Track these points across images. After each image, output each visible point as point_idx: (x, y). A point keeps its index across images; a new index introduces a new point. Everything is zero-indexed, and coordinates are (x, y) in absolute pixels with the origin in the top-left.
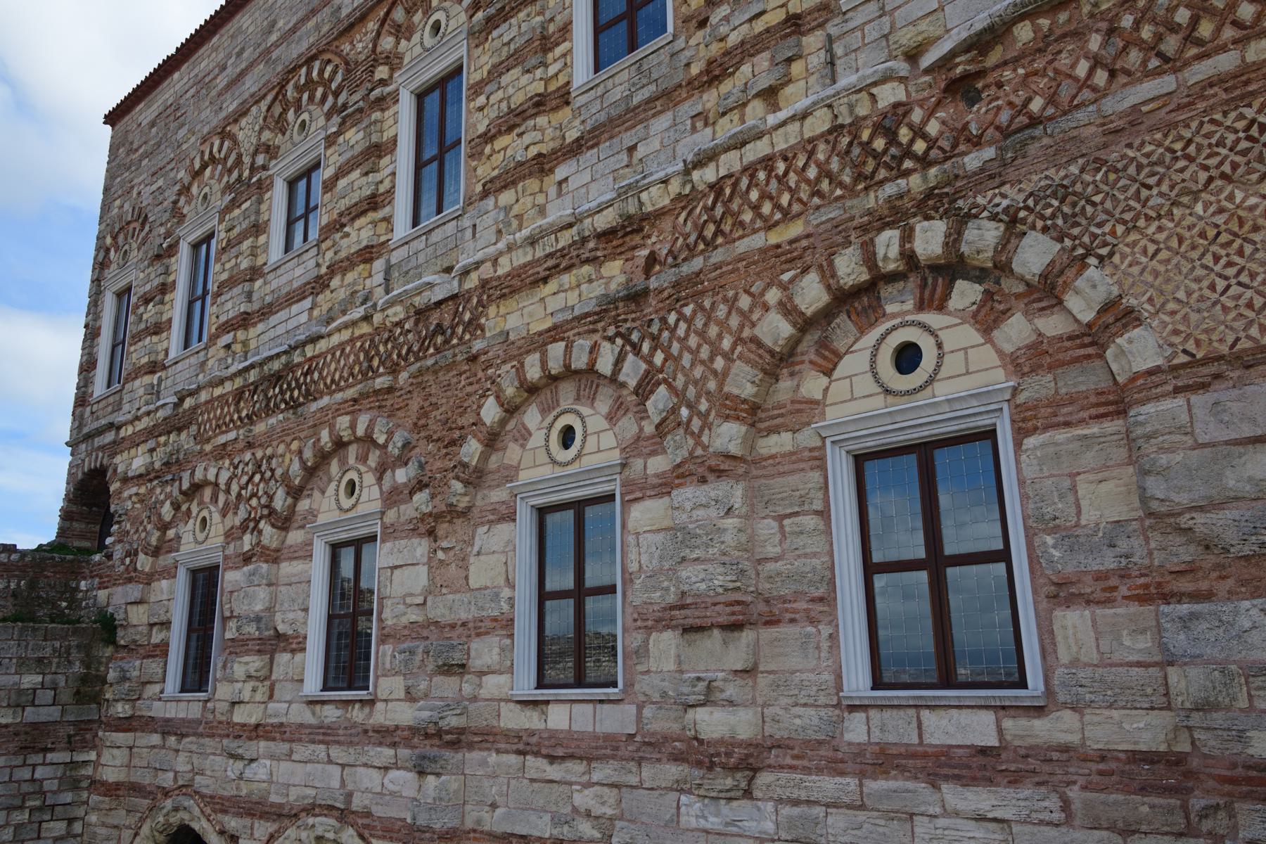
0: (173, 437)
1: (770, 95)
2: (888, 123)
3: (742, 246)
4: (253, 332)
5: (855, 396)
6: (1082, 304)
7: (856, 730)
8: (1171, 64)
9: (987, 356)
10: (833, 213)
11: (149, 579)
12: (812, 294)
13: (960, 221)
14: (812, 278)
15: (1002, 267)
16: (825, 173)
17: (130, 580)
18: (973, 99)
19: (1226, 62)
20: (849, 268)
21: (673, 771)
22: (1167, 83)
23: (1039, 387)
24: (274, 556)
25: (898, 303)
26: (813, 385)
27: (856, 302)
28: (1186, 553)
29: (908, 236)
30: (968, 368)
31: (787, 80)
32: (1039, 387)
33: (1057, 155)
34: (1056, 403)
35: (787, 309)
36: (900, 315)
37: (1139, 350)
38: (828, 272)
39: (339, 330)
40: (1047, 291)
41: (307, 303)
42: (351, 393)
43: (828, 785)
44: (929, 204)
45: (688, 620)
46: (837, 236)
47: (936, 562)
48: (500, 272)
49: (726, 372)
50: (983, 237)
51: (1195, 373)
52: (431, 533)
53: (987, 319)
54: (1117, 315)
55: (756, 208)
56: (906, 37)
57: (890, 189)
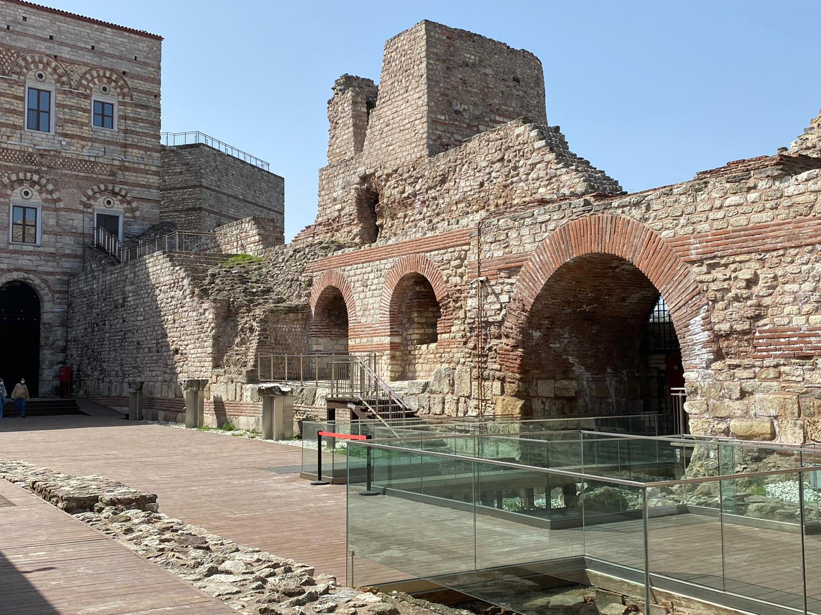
2: (31, 155)
5: (16, 196)
6: (55, 196)
7: (11, 247)
8: (70, 170)
9: (39, 198)
10: (19, 165)
12: (14, 177)
13: (41, 177)
14: (14, 175)
15: (45, 186)
16: (18, 157)
18: (42, 158)
19: (76, 173)
20: (21, 176)
22: (70, 172)
23: (46, 204)
25: (26, 185)
26: (9, 192)
27: (20, 182)
28: (61, 230)
29: (32, 175)
30: (36, 198)
32: (46, 204)
33: (56, 174)
34: (48, 208)
35: (9, 178)
36: (26, 187)
37: (62, 205)
38: (18, 175)
40: (51, 192)
43: (5, 255)
44: (37, 172)
46: (20, 170)
47: (24, 225)
50: (44, 181)
51: (67, 210)
53: (40, 192)
54: (59, 200)
56: (35, 142)
57: (30, 167)
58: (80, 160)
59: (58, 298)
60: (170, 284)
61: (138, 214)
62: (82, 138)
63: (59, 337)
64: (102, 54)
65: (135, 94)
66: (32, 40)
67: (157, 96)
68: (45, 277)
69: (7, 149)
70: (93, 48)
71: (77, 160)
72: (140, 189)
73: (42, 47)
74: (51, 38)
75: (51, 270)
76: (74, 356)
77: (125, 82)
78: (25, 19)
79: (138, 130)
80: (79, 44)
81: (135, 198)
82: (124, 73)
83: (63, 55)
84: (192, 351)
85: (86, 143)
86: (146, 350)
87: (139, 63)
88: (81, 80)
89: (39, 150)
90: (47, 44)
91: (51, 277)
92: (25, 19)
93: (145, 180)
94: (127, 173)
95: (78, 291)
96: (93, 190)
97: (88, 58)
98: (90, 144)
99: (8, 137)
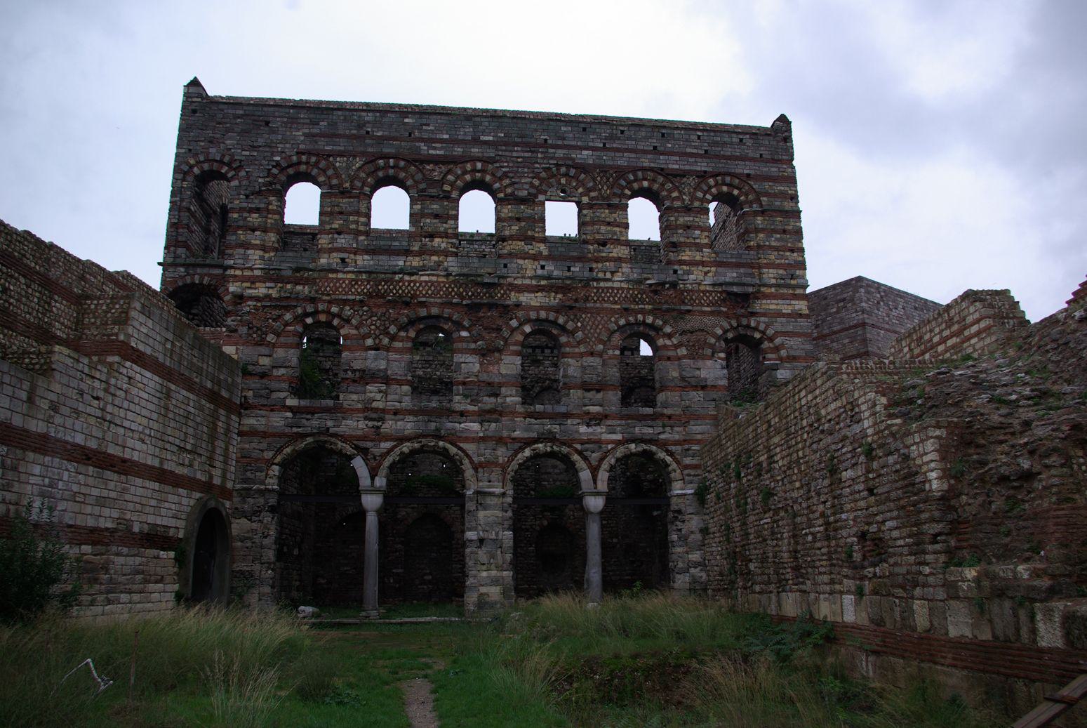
0: (289, 286)
1: (613, 273)
3: (606, 305)
4: (359, 258)
11: (274, 346)
16: (626, 296)
17: (260, 345)
21: (578, 421)
24: (388, 349)
31: (618, 272)
35: (616, 323)
39: (428, 275)
41: (403, 258)
42: (439, 301)
45: (586, 387)
48: (516, 282)
49: (599, 334)
52: (484, 355)
55: (609, 297)
58: (703, 292)
59: (689, 475)
60: (839, 416)
61: (783, 353)
62: (703, 263)
63: (694, 529)
64: (718, 157)
65: (765, 199)
66: (633, 155)
67: (794, 198)
68: (670, 448)
69: (613, 288)
70: (706, 151)
71: (699, 291)
72: (784, 320)
73: (645, 162)
74: (655, 148)
75: (677, 437)
76: (715, 553)
77: (750, 185)
78: (622, 132)
79: (773, 244)
80: (689, 150)
81: (777, 334)
82: (748, 175)
83: (670, 166)
84: (895, 534)
85: (708, 268)
86: (810, 538)
87: (767, 161)
88: (695, 192)
89: (651, 285)
90: (649, 156)
91: (679, 448)
92: (622, 132)
93: (790, 308)
94: (764, 301)
95: (711, 462)
96: (722, 327)
97: (702, 166)
98: (713, 269)
99: (613, 273)
